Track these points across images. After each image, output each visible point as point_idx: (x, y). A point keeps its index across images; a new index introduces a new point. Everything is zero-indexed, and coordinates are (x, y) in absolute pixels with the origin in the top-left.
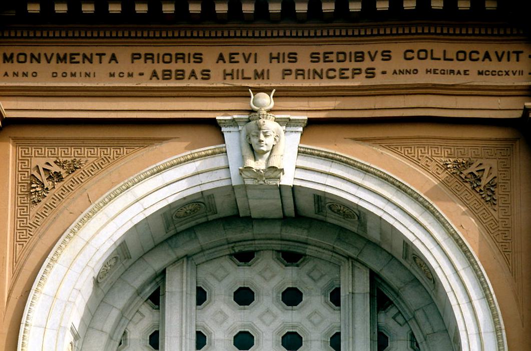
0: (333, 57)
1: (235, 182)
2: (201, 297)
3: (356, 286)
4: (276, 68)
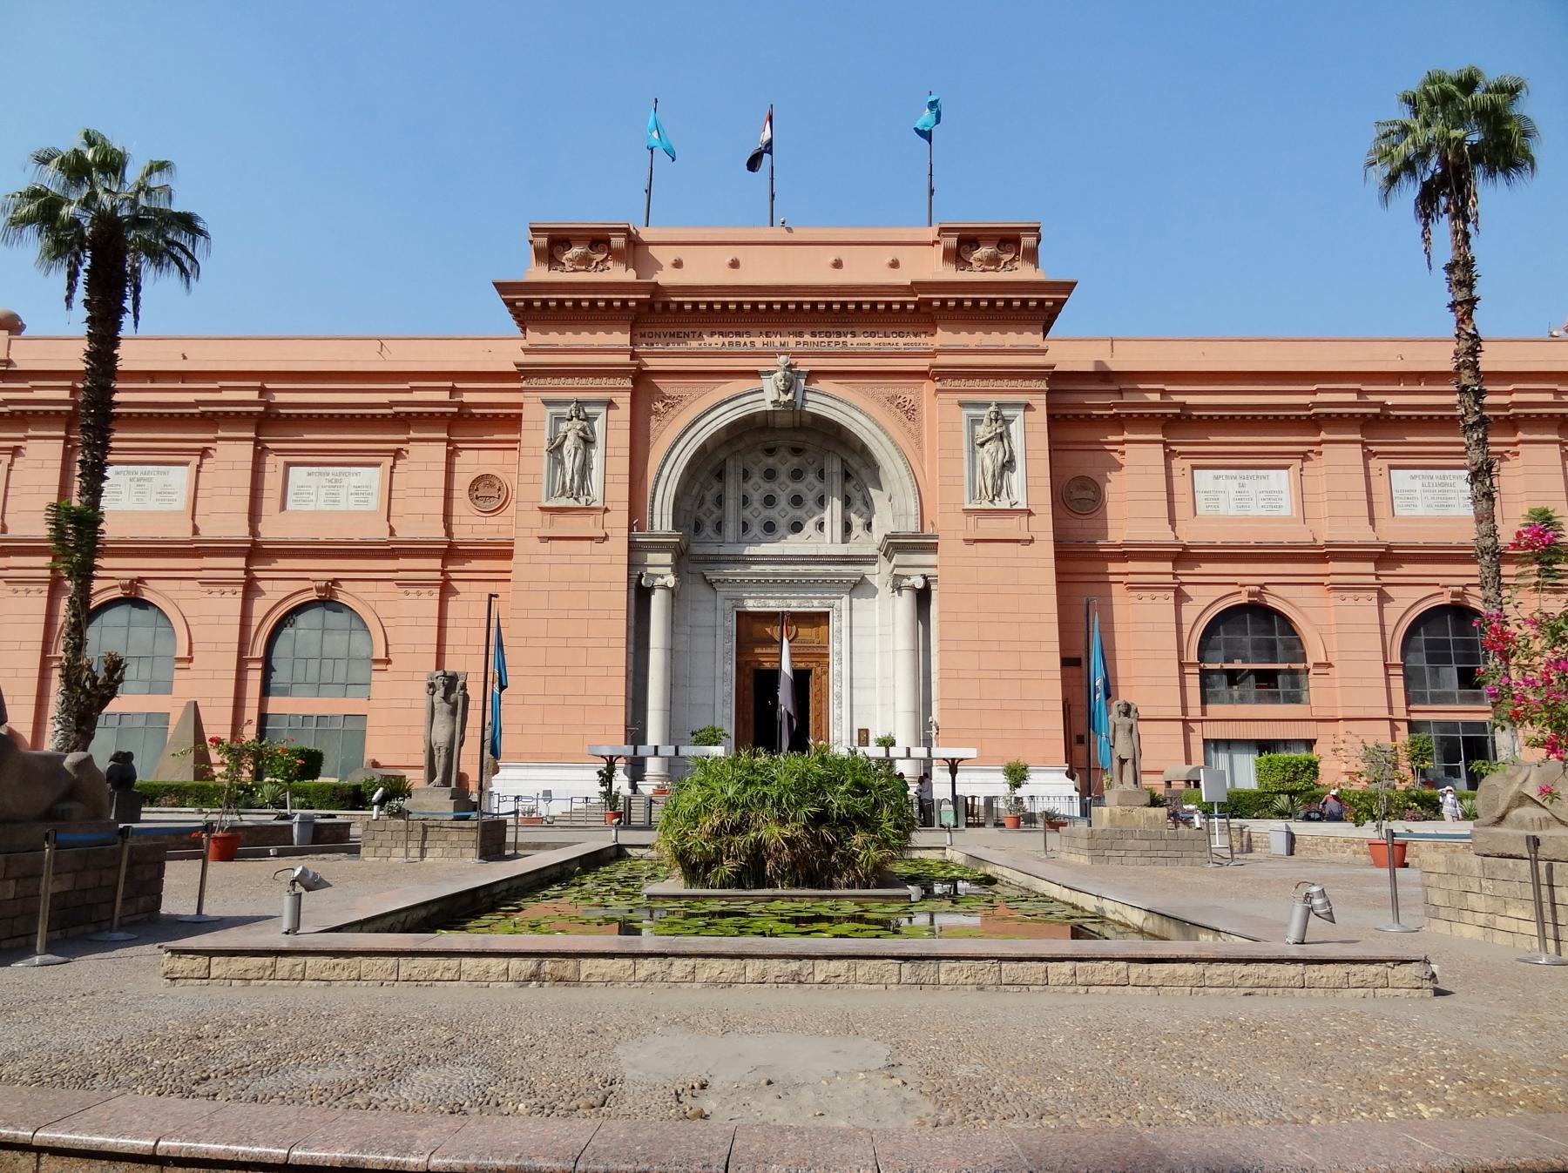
1: (770, 408)
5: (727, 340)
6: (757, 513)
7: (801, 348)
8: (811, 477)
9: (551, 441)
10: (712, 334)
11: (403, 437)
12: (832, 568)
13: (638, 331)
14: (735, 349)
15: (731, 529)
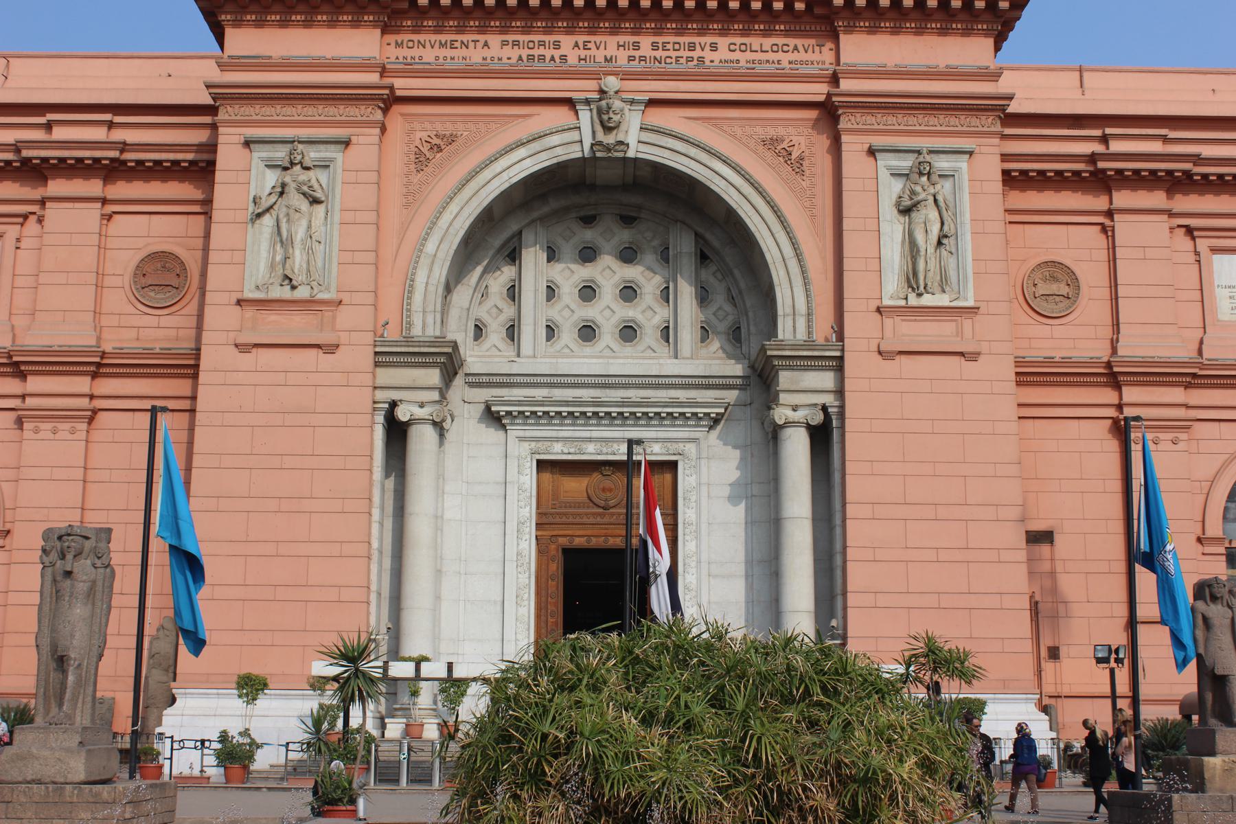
0: (669, 46)
2: (552, 256)
3: (684, 244)
4: (622, 57)
5: (525, 53)
6: (570, 312)
7: (636, 66)
9: (255, 201)
10: (504, 43)
11: (37, 193)
12: (682, 395)
13: (391, 38)
14: (538, 66)
15: (530, 332)
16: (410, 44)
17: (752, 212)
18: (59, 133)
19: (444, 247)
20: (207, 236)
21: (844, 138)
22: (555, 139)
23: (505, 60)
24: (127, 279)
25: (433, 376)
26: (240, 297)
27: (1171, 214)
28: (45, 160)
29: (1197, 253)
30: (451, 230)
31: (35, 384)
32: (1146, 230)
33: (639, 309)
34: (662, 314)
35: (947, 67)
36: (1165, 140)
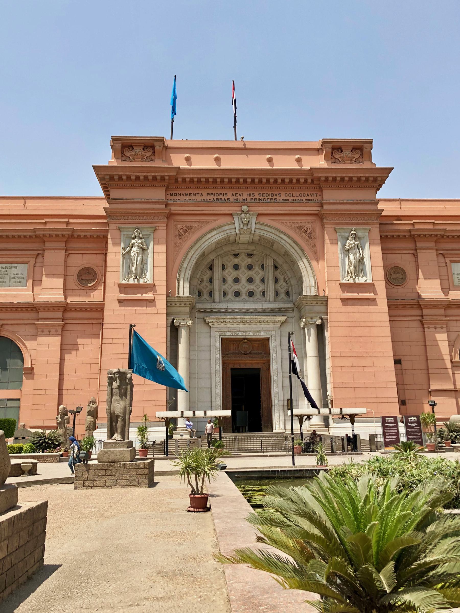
1: (238, 232)
2: (224, 267)
4: (249, 198)
5: (215, 198)
6: (231, 287)
8: (257, 268)
13: (169, 193)
15: (217, 296)
16: (175, 195)
17: (294, 252)
18: (49, 226)
19: (190, 264)
20: (105, 261)
21: (325, 226)
22: (226, 228)
23: (208, 200)
24: (75, 277)
25: (187, 309)
26: (119, 283)
27: (437, 250)
28: (44, 235)
29: (446, 263)
30: (192, 260)
31: (42, 314)
32: (427, 256)
33: (255, 285)
34: (262, 287)
35: (360, 200)
36: (434, 224)
